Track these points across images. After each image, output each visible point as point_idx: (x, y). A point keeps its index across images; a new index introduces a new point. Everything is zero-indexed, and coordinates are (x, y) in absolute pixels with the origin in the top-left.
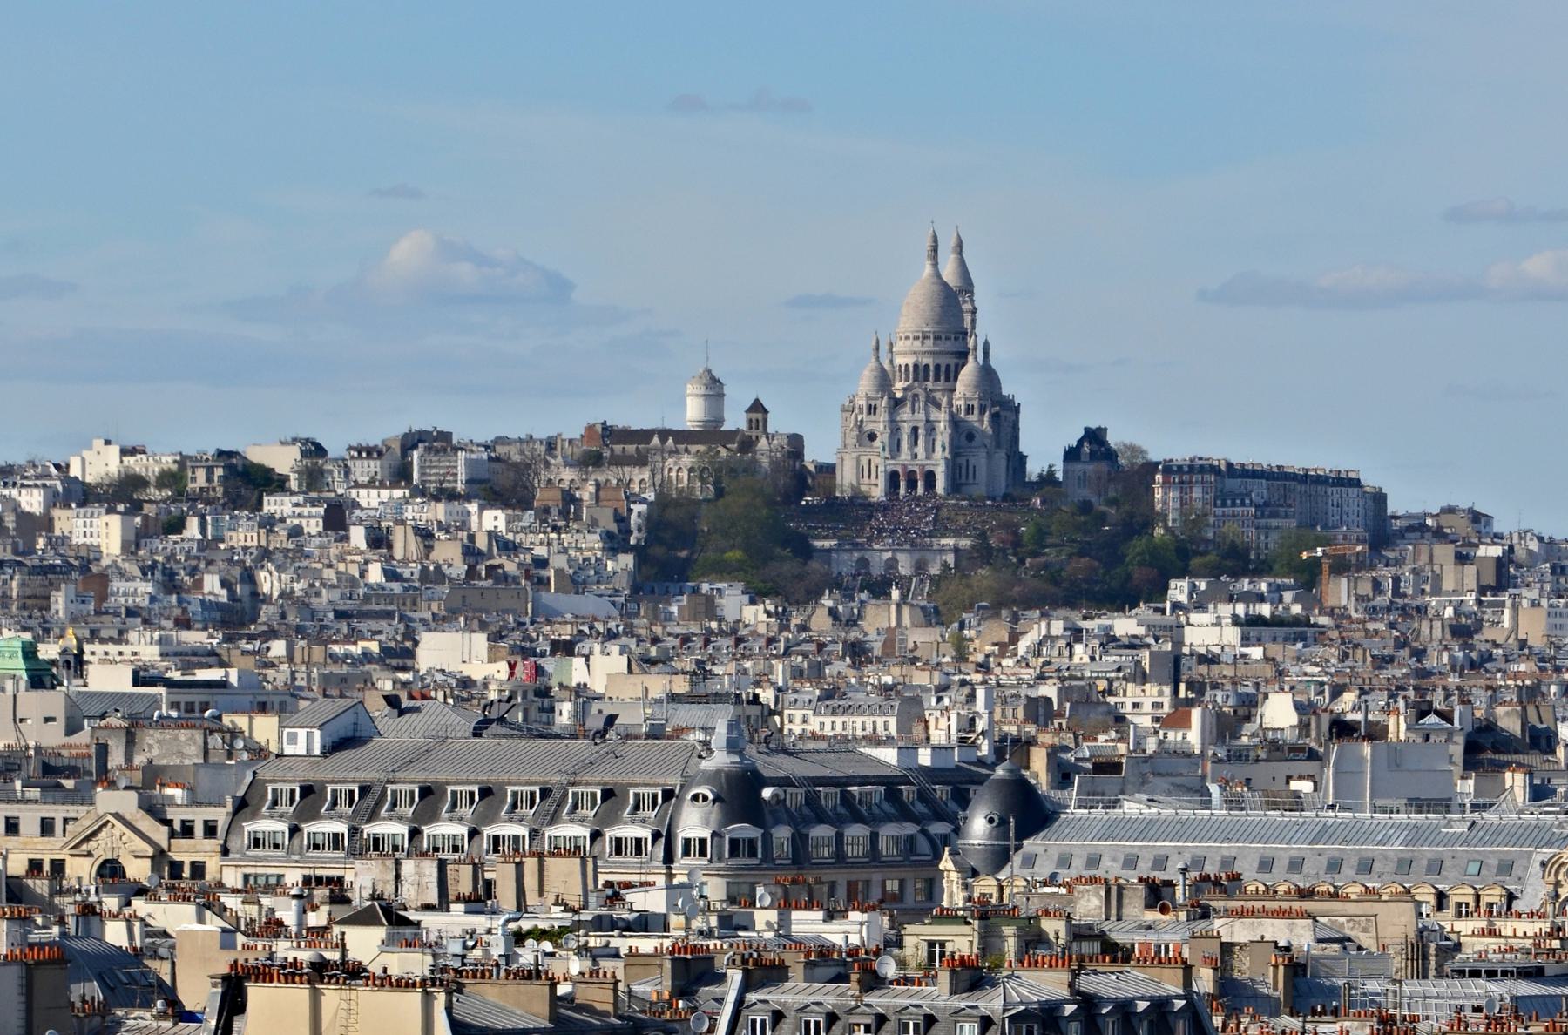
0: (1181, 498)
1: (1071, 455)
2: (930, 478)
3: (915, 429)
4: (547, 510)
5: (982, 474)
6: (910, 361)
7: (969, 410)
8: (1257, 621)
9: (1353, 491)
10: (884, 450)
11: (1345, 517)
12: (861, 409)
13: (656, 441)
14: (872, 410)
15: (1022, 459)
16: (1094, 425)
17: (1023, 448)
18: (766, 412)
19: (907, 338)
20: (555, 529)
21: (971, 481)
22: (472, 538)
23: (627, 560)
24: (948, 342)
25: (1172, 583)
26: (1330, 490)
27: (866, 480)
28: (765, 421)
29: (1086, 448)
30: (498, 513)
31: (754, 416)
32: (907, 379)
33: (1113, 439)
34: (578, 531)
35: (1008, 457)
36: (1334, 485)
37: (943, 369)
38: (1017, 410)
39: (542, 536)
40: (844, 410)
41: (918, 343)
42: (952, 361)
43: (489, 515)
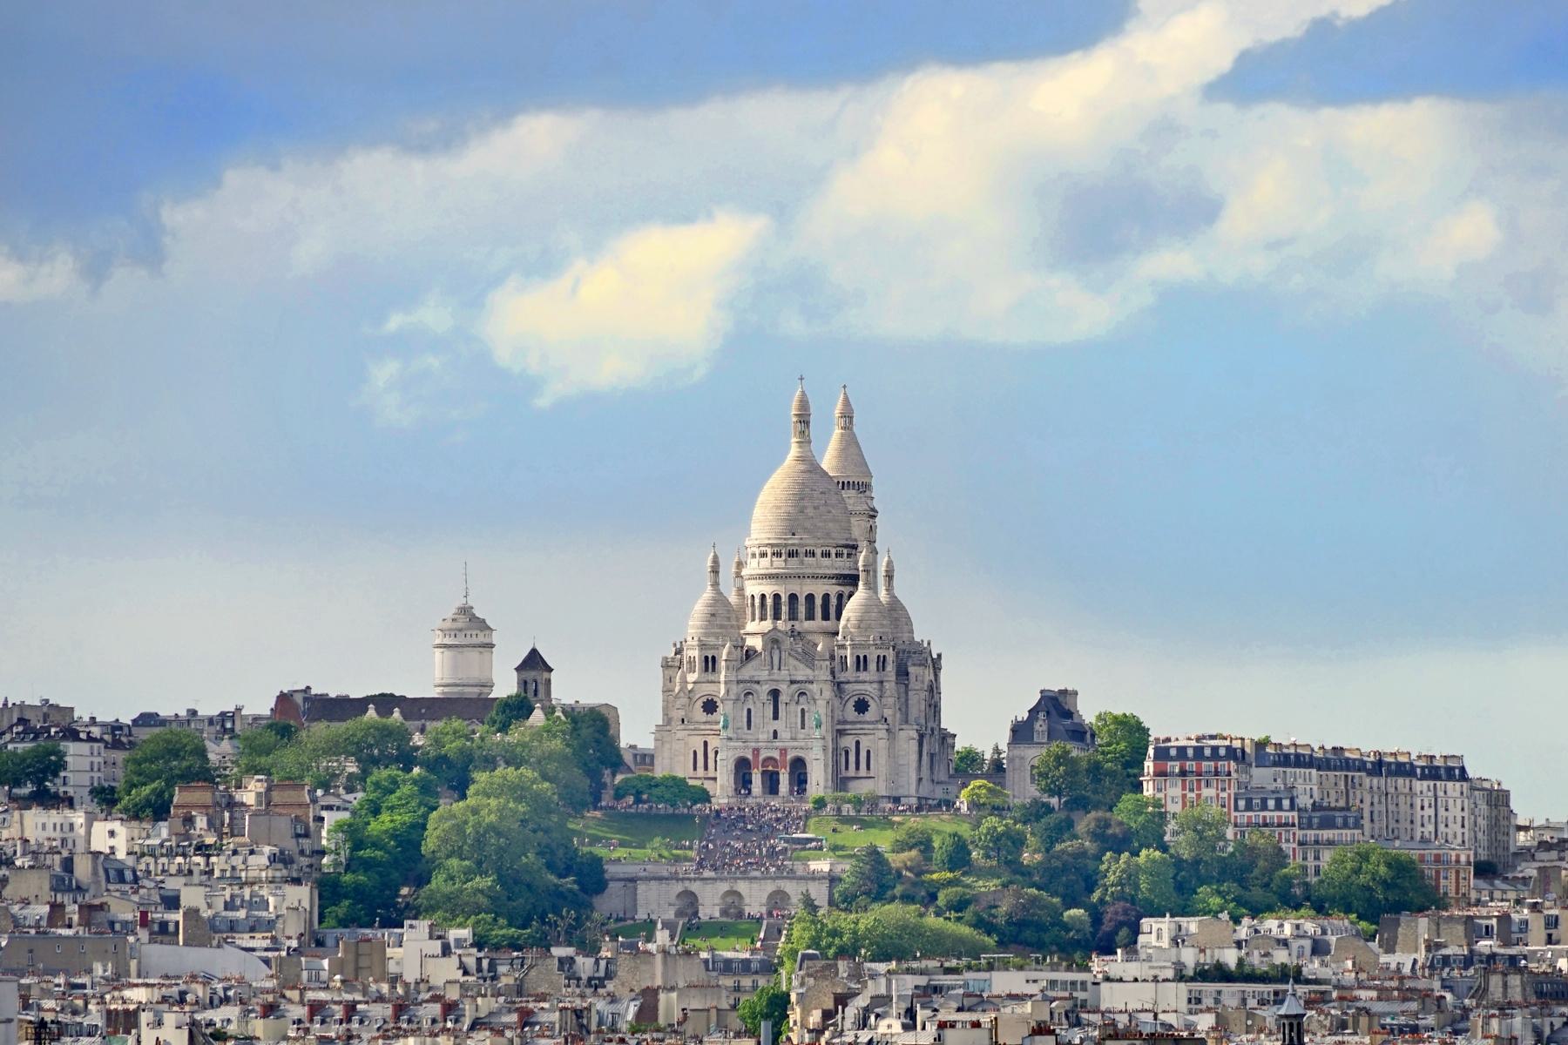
0: (1184, 796)
1: (1021, 733)
2: (798, 767)
3: (775, 694)
4: (189, 821)
5: (880, 764)
6: (769, 589)
7: (862, 663)
8: (1220, 974)
9: (1454, 788)
10: (725, 727)
11: (1442, 827)
12: (691, 662)
13: (371, 713)
14: (710, 663)
15: (946, 738)
16: (1056, 687)
17: (947, 723)
18: (551, 670)
19: (763, 555)
20: (202, 849)
21: (863, 772)
22: (68, 865)
23: (302, 895)
24: (826, 561)
25: (1146, 923)
26: (1419, 786)
27: (700, 772)
28: (548, 682)
29: (1041, 726)
30: (116, 826)
31: (530, 675)
32: (777, 617)
33: (1088, 711)
34: (235, 852)
35: (921, 736)
36: (1423, 778)
37: (818, 602)
38: (936, 665)
39: (180, 860)
40: (666, 665)
41: (779, 562)
42: (833, 590)
43: (100, 828)
